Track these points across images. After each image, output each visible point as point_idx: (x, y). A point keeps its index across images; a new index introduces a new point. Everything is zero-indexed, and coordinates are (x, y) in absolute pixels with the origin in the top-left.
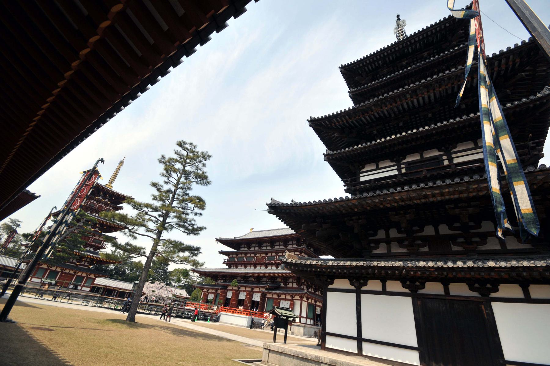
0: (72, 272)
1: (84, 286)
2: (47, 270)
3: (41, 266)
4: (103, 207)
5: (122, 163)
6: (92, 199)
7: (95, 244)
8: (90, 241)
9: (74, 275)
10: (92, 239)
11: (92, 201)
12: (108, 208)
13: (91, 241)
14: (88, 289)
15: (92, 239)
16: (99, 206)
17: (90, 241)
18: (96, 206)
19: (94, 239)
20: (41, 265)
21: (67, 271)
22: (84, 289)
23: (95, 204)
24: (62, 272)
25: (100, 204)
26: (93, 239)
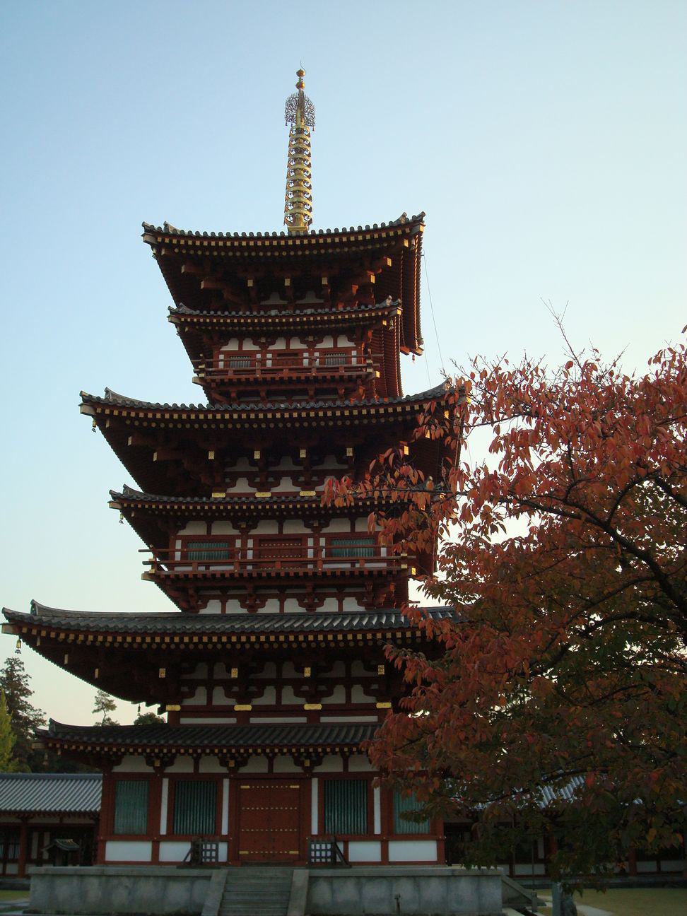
0: (285, 766)
1: (389, 835)
2: (152, 782)
3: (117, 769)
4: (297, 353)
5: (299, 109)
6: (225, 337)
7: (348, 566)
8: (310, 553)
9: (304, 780)
10: (316, 542)
11: (232, 346)
12: (327, 344)
13: (316, 554)
14: (426, 851)
15: (316, 542)
16: (279, 354)
17: (310, 553)
18: (263, 362)
19: (331, 538)
20: (118, 763)
21: (257, 766)
22: (401, 851)
23: (253, 353)
24: (237, 780)
25: (280, 346)
26: (323, 542)
